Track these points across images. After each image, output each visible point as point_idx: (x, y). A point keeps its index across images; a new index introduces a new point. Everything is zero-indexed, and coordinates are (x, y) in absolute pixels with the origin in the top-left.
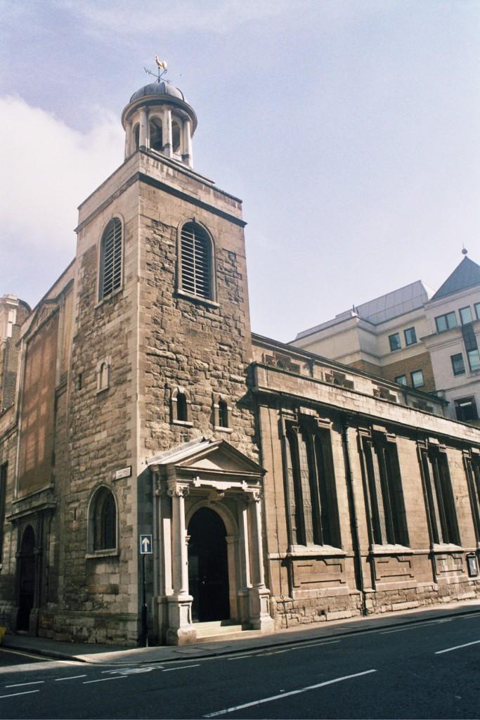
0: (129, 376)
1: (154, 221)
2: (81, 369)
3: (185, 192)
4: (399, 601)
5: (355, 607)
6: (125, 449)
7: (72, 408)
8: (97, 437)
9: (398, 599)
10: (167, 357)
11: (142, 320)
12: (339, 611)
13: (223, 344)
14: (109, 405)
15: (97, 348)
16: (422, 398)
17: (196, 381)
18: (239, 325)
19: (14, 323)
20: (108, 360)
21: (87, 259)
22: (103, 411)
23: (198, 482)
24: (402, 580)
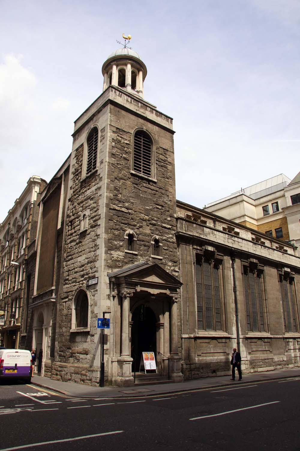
0: (99, 222)
1: (117, 128)
2: (73, 217)
3: (138, 112)
4: (262, 366)
6: (95, 267)
7: (66, 241)
8: (79, 259)
9: (261, 365)
10: (123, 212)
11: (108, 188)
12: (224, 371)
13: (158, 205)
14: (87, 240)
15: (82, 205)
16: (282, 244)
17: (141, 227)
18: (168, 194)
19: (38, 192)
20: (87, 212)
21: (78, 151)
22: (83, 243)
23: (139, 289)
24: (264, 354)
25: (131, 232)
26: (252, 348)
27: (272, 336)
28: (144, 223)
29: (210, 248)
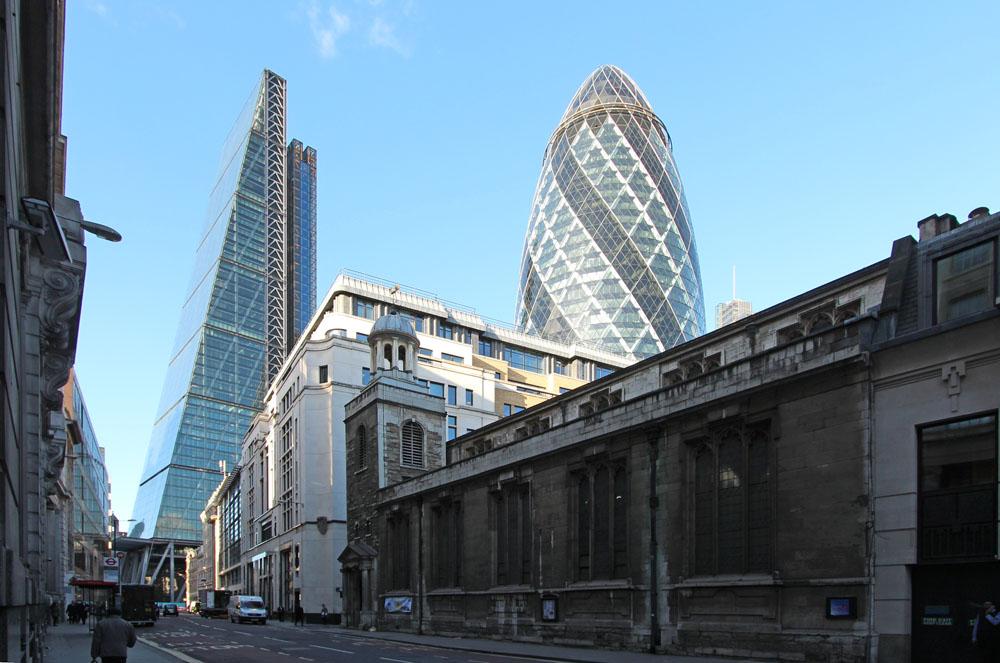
29: (396, 508)
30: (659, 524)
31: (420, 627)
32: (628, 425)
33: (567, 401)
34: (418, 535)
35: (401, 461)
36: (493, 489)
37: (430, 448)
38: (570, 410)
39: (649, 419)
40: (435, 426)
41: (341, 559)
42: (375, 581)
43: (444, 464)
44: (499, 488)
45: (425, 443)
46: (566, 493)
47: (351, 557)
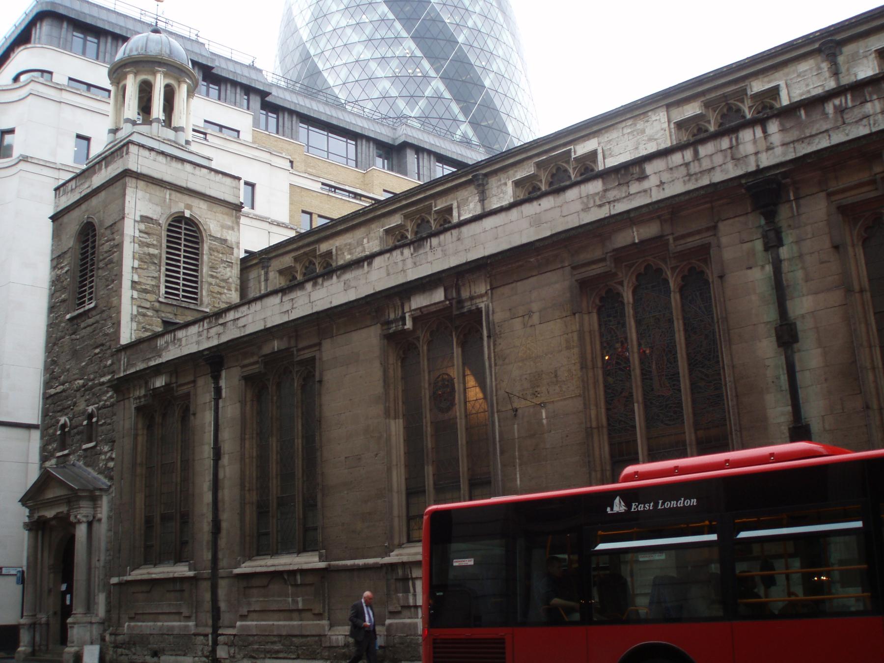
5: (200, 653)
9: (278, 652)
24: (291, 620)
25: (63, 420)
26: (249, 604)
27: (322, 565)
28: (78, 394)
29: (160, 382)
30: (804, 378)
31: (214, 651)
32: (705, 181)
33: (486, 175)
34: (209, 437)
35: (163, 290)
36: (393, 328)
37: (212, 268)
38: (494, 191)
39: (752, 168)
40: (223, 227)
41: (24, 501)
42: (103, 545)
43: (234, 297)
44: (409, 325)
45: (205, 258)
46: (576, 327)
47: (52, 493)
